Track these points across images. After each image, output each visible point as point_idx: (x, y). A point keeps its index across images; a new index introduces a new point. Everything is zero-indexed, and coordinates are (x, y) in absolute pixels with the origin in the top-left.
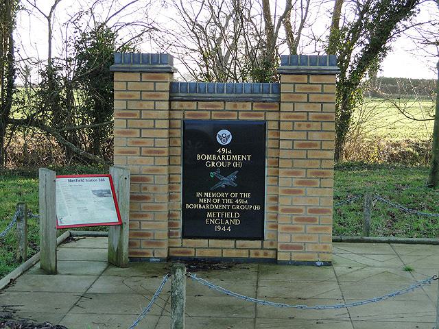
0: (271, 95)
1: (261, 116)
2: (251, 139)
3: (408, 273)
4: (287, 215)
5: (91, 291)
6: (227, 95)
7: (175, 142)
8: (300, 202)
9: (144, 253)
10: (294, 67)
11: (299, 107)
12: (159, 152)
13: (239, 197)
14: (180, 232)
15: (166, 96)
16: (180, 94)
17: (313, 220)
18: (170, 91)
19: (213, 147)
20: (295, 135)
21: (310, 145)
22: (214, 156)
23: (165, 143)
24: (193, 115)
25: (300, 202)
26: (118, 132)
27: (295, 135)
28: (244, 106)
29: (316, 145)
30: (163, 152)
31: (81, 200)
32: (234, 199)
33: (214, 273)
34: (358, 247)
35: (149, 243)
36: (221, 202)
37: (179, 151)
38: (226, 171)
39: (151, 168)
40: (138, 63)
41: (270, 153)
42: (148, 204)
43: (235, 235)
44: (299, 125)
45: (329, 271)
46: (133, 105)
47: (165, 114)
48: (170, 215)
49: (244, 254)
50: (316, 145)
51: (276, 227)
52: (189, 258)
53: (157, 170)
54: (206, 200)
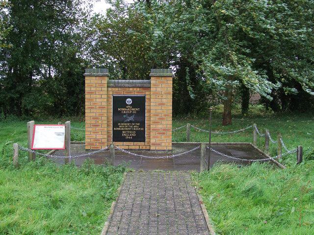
13: (135, 125)
17: (164, 133)
19: (125, 105)
25: (160, 126)
36: (128, 127)
38: (130, 115)
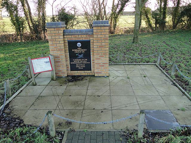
0: (91, 33)
1: (89, 38)
2: (86, 45)
3: (128, 79)
4: (97, 65)
5: (41, 95)
6: (79, 33)
7: (66, 47)
8: (100, 61)
9: (61, 75)
10: (97, 25)
11: (99, 36)
12: (62, 50)
13: (84, 60)
14: (70, 69)
15: (62, 34)
16: (66, 34)
17: (104, 66)
18: (63, 33)
19: (76, 48)
20: (98, 44)
21: (102, 46)
22: (77, 50)
23: (63, 47)
24: (70, 39)
25: (100, 61)
26: (50, 45)
27: (98, 44)
28: (84, 36)
29: (104, 46)
30: (63, 50)
31: (41, 66)
32: (83, 61)
33: (78, 82)
34: (116, 67)
35: (62, 73)
36: (80, 62)
37: (68, 49)
38: (80, 54)
39: (60, 54)
40: (53, 25)
41: (91, 49)
42: (59, 63)
43: (84, 69)
44: (99, 41)
45: (107, 80)
46: (53, 37)
47: (62, 39)
48: (67, 65)
49: (87, 74)
50: (104, 46)
51: (94, 67)
52: (73, 76)
53: (62, 55)
54: (76, 61)
